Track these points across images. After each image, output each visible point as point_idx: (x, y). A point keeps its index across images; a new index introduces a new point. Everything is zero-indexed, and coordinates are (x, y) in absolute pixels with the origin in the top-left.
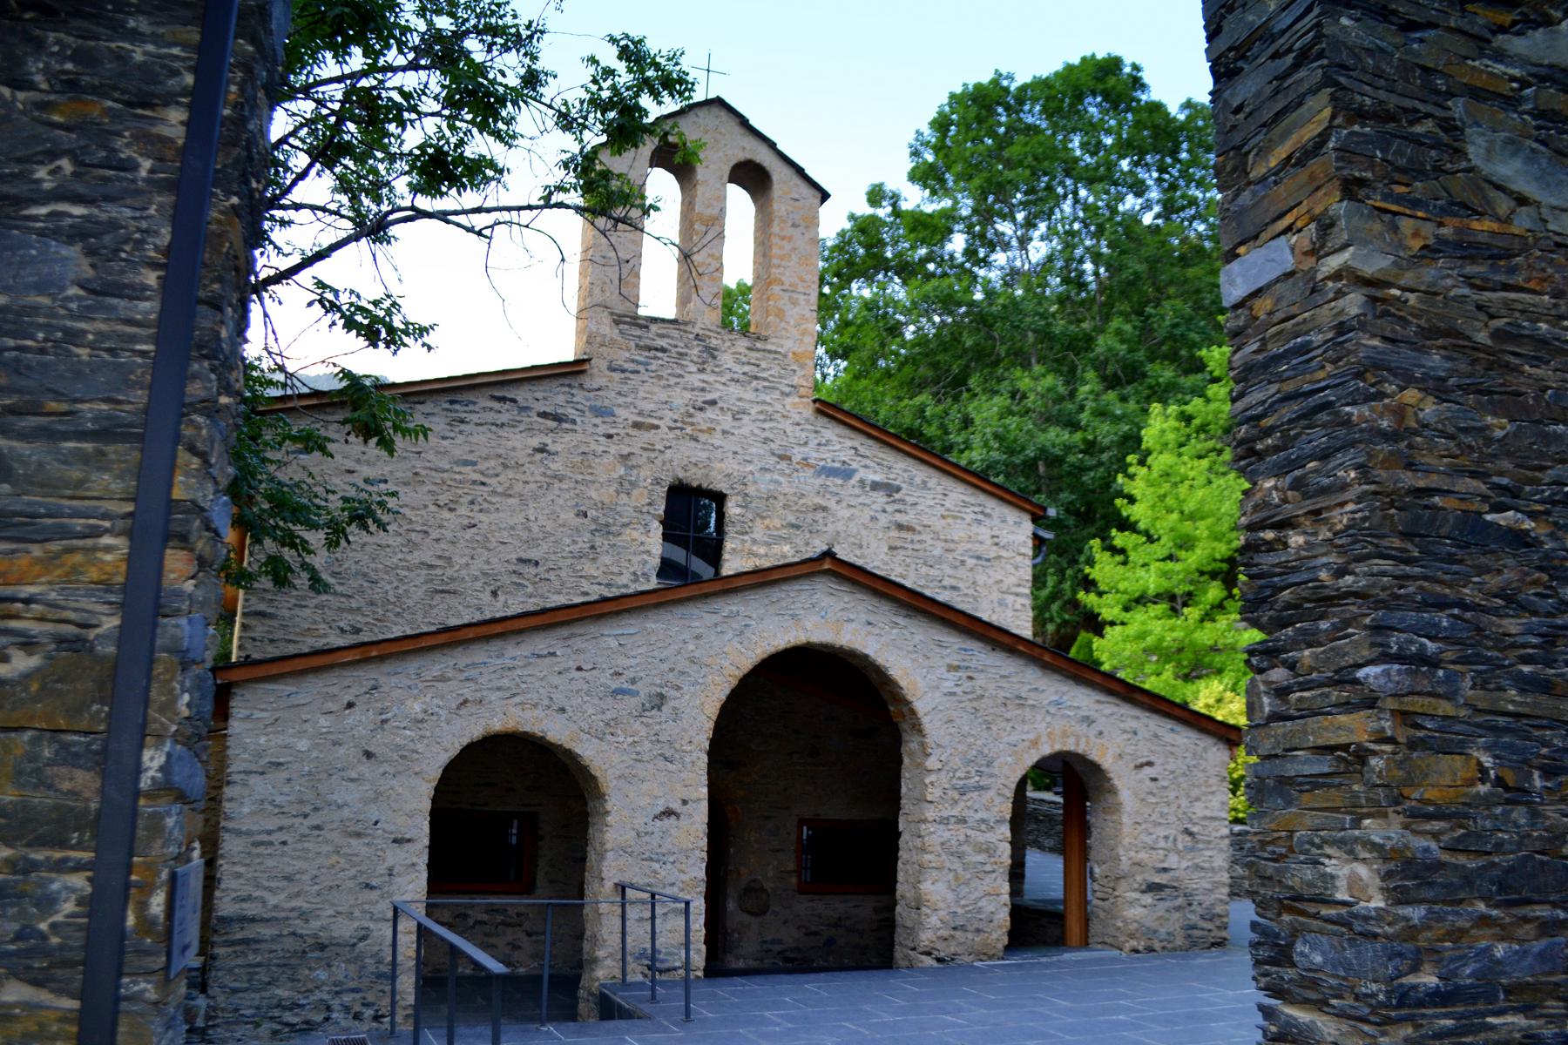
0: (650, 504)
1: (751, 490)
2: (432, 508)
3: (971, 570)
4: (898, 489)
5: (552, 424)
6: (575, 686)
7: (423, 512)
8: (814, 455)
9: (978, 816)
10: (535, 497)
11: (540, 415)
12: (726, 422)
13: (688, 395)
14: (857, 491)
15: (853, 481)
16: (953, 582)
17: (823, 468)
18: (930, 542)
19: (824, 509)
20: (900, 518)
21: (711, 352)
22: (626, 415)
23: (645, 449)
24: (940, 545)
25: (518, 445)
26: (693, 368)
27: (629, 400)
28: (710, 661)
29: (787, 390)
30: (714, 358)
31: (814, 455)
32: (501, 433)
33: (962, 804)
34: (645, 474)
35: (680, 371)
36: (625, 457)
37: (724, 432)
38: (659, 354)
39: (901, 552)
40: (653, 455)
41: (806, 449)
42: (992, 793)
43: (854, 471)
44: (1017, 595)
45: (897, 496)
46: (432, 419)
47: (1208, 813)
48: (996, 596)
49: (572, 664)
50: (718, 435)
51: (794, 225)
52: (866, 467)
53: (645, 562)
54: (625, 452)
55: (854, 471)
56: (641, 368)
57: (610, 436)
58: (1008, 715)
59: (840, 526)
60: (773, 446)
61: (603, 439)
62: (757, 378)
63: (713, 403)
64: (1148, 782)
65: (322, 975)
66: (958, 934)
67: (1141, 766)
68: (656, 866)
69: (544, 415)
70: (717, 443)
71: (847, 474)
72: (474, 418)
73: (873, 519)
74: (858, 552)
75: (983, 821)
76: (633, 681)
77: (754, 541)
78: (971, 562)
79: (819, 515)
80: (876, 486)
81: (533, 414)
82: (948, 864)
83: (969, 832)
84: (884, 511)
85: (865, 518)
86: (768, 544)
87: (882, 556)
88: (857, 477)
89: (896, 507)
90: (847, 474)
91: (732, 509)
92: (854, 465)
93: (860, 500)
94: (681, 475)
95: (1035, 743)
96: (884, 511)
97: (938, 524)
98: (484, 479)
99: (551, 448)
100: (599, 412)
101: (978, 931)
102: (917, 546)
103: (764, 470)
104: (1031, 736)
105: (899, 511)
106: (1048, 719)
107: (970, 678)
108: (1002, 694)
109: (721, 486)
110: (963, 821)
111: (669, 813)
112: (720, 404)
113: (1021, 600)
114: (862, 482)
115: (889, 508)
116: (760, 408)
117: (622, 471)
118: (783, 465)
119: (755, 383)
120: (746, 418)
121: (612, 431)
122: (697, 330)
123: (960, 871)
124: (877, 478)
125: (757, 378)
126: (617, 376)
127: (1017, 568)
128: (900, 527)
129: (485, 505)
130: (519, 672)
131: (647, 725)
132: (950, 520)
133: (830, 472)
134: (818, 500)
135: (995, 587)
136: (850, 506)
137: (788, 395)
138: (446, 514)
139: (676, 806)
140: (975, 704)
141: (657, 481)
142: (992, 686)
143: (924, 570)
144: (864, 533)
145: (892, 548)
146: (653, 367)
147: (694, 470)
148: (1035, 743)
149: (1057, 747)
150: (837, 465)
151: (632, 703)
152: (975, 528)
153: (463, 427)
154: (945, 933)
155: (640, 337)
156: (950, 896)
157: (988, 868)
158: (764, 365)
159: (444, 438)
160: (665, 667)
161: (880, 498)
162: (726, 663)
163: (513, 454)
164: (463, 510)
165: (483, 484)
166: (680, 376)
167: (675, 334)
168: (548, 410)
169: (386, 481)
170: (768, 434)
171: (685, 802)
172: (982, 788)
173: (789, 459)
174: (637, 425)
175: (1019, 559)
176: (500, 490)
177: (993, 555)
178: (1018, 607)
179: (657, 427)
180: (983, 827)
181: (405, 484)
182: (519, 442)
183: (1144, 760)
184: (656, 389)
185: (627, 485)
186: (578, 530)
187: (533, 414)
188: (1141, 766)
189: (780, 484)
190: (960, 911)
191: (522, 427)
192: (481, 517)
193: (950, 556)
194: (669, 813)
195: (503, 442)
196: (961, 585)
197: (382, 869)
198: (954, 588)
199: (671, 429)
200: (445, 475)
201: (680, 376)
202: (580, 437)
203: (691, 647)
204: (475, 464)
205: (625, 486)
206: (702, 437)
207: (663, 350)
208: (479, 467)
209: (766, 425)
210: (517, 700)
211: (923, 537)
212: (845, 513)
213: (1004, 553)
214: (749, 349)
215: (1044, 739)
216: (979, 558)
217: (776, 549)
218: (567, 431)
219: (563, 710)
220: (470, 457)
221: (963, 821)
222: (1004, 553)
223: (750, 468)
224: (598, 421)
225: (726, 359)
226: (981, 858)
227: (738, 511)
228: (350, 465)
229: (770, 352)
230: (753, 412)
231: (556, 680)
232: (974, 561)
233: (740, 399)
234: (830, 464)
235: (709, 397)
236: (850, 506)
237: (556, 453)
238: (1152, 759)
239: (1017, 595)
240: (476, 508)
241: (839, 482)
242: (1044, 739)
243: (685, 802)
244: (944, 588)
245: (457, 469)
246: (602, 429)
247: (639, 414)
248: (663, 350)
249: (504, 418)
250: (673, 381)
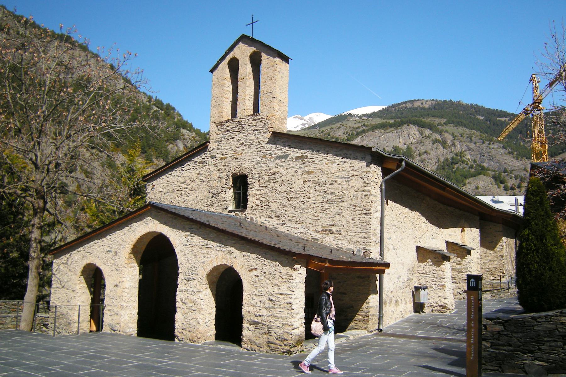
0: (226, 184)
1: (254, 172)
2: (177, 198)
3: (340, 184)
4: (307, 157)
5: (201, 165)
6: (102, 250)
7: (175, 200)
8: (274, 152)
9: (191, 289)
10: (198, 189)
11: (200, 163)
12: (246, 149)
13: (235, 144)
14: (290, 162)
15: (288, 159)
16: (332, 191)
17: (277, 157)
18: (321, 176)
19: (277, 173)
20: (308, 169)
21: (242, 125)
22: (219, 156)
23: (224, 166)
24: (325, 176)
25: (193, 174)
26: (237, 133)
27: (220, 151)
28: (127, 240)
29: (265, 131)
30: (243, 128)
31: (274, 152)
32: (190, 171)
33: (188, 285)
34: (223, 175)
35: (234, 136)
36: (219, 170)
37: (245, 153)
38: (228, 132)
39: (308, 183)
40: (226, 167)
41: (270, 152)
42: (196, 281)
43: (288, 155)
44: (363, 191)
45: (305, 160)
46: (177, 172)
47: (280, 292)
48: (352, 193)
49: (102, 245)
50: (243, 155)
51: (268, 68)
52: (293, 152)
53: (225, 204)
54: (219, 169)
55: (288, 155)
56: (223, 139)
57: (215, 164)
58: (203, 252)
59: (283, 178)
60: (260, 153)
61: (213, 166)
62: (256, 130)
63: (242, 144)
64: (254, 277)
65: (62, 321)
66: (184, 331)
67: (252, 270)
68: (113, 300)
69: (200, 163)
70: (243, 158)
71: (286, 156)
72: (185, 169)
73: (296, 172)
74: (291, 187)
75: (193, 291)
76: (111, 248)
77: (256, 190)
78: (339, 181)
79: (276, 176)
80: (298, 158)
81: (197, 163)
82: (182, 306)
83: (189, 295)
84: (301, 167)
85: (293, 173)
86: (260, 190)
87: (300, 186)
88: (290, 157)
89: (306, 164)
90: (286, 156)
91: (249, 180)
92: (289, 152)
93: (291, 166)
94: (234, 172)
95: (211, 262)
96: (301, 167)
97: (324, 168)
98: (187, 187)
99: (201, 173)
100: (213, 157)
101: (190, 331)
102: (316, 179)
103: (257, 164)
104: (210, 259)
105: (307, 166)
106: (217, 252)
107: (192, 239)
108: (201, 244)
109: (245, 172)
110: (187, 291)
111: (116, 286)
112: (245, 143)
113: (364, 193)
114: (292, 158)
115: (302, 166)
116: (256, 141)
117: (218, 174)
118: (264, 159)
119: (255, 132)
120: (252, 146)
121: (216, 162)
122: (238, 120)
123: (185, 309)
124: (298, 155)
125: (256, 130)
126: (217, 144)
127: (363, 178)
128: (308, 172)
129: (188, 194)
130: (92, 248)
131: (113, 260)
132: (329, 165)
133: (279, 157)
134: (275, 170)
135: (352, 189)
136: (287, 169)
137: (266, 132)
138: (179, 199)
139: (118, 283)
140: (193, 248)
141: (227, 176)
142: (198, 241)
143: (318, 188)
144: (293, 178)
145: (304, 182)
146: (226, 137)
147: (237, 169)
148: (211, 262)
149: (219, 263)
150: (283, 154)
151: (111, 254)
152: (342, 165)
153: (183, 172)
154: (180, 331)
155: (223, 129)
156: (182, 318)
157: (194, 309)
158: (258, 125)
159: (179, 177)
160: (118, 243)
161: (299, 163)
162: (130, 241)
163: (192, 177)
164: (183, 197)
165: (187, 188)
166: (234, 138)
167: (232, 124)
168: (200, 161)
169: (168, 193)
170: (259, 149)
171: (119, 282)
172: (193, 279)
173: (266, 156)
174: (222, 159)
175: (364, 174)
176: (190, 189)
177: (351, 175)
178: (363, 196)
179: (227, 157)
180: (193, 293)
181: (172, 192)
182: (194, 172)
183: (253, 268)
184: (227, 145)
185: (220, 179)
186: (208, 197)
187: (197, 163)
188: (252, 270)
189: (261, 166)
190: (185, 323)
191: (195, 168)
192: (187, 198)
193: (330, 180)
194: (116, 286)
195: (191, 174)
196: (336, 192)
197: (70, 298)
198: (332, 193)
199: (230, 157)
200: (179, 188)
201: (234, 138)
202: (207, 167)
203: (123, 237)
204: (184, 182)
205: (219, 179)
206: (239, 157)
207: (229, 131)
208: (186, 183)
209: (258, 147)
210: (91, 255)
211: (318, 174)
212: (284, 172)
213: (356, 173)
214: (253, 120)
215: (215, 260)
216: (344, 178)
217: (263, 191)
218: (205, 166)
219: (99, 257)
220: (184, 181)
221: (187, 291)
222: (356, 173)
223: (254, 163)
224: (212, 160)
225: (246, 126)
226: (192, 305)
227: (251, 180)
228: (161, 189)
229: (259, 119)
230: (254, 143)
231: (98, 249)
232: (342, 180)
233: (250, 140)
234: (280, 154)
235: (241, 142)
236: (287, 169)
237: (202, 174)
238: (256, 267)
239: (363, 191)
240: (186, 195)
241: (283, 160)
242: (215, 260)
243: (119, 282)
244: (328, 194)
245: (181, 185)
246: (213, 163)
247: (222, 155)
248: (229, 131)
249: (191, 167)
250: (231, 140)
